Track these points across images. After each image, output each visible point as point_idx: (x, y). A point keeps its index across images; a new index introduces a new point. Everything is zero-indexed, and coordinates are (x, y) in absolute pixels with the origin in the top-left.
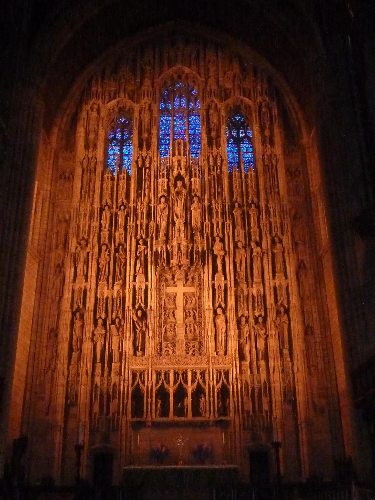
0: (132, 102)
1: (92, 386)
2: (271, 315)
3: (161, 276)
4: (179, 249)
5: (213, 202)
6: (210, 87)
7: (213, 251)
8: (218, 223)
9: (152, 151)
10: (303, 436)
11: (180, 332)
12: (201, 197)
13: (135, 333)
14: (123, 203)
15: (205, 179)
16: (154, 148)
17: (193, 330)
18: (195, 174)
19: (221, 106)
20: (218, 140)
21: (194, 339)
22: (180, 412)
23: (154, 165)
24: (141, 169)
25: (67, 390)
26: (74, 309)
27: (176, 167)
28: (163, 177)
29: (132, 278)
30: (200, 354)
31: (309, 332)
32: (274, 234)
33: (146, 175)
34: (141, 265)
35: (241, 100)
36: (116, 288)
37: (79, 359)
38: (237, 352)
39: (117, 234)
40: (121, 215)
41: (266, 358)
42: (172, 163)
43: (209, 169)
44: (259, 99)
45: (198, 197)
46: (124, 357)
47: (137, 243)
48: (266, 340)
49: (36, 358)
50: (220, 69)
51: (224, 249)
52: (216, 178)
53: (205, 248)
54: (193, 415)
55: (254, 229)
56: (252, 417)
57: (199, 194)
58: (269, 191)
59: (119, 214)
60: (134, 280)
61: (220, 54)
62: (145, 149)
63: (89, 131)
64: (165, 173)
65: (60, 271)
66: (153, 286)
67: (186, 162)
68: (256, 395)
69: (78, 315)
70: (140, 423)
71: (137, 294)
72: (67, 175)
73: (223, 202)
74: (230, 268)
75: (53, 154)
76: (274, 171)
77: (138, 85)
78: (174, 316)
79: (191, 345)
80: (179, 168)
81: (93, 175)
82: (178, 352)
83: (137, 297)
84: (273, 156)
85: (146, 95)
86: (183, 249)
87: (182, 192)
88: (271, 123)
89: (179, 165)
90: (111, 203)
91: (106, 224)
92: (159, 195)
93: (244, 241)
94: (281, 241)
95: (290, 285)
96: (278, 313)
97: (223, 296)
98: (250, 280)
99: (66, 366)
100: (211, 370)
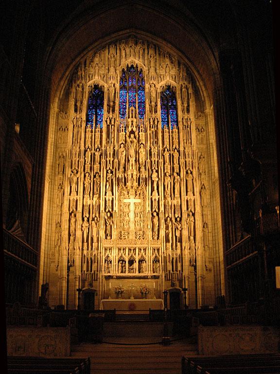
1: (82, 255)
2: (185, 216)
3: (121, 192)
4: (132, 177)
5: (152, 148)
7: (152, 178)
8: (155, 161)
10: (199, 284)
11: (132, 225)
13: (106, 226)
17: (139, 225)
18: (142, 130)
21: (140, 230)
25: (68, 258)
26: (70, 212)
28: (122, 131)
29: (104, 194)
30: (143, 239)
31: (205, 227)
32: (187, 168)
34: (109, 185)
37: (74, 240)
38: (165, 238)
39: (95, 166)
40: (97, 154)
41: (181, 241)
43: (150, 127)
44: (181, 83)
45: (143, 144)
46: (100, 240)
47: (107, 172)
48: (181, 231)
49: (50, 239)
50: (157, 61)
51: (158, 177)
53: (147, 176)
54: (139, 272)
55: (176, 166)
56: (172, 274)
57: (144, 143)
58: (185, 141)
59: (96, 154)
60: (105, 195)
62: (111, 113)
65: (62, 188)
66: (116, 199)
68: (174, 261)
69: (73, 214)
71: (107, 203)
74: (161, 188)
75: (55, 115)
76: (189, 129)
78: (128, 216)
79: (138, 233)
82: (131, 237)
83: (107, 205)
84: (188, 119)
85: (112, 78)
86: (135, 177)
88: (188, 99)
89: (132, 124)
91: (88, 159)
92: (120, 143)
93: (170, 172)
94: (191, 173)
95: (196, 199)
96: (188, 215)
97: (157, 205)
98: (173, 195)
99: (67, 244)
100: (149, 248)
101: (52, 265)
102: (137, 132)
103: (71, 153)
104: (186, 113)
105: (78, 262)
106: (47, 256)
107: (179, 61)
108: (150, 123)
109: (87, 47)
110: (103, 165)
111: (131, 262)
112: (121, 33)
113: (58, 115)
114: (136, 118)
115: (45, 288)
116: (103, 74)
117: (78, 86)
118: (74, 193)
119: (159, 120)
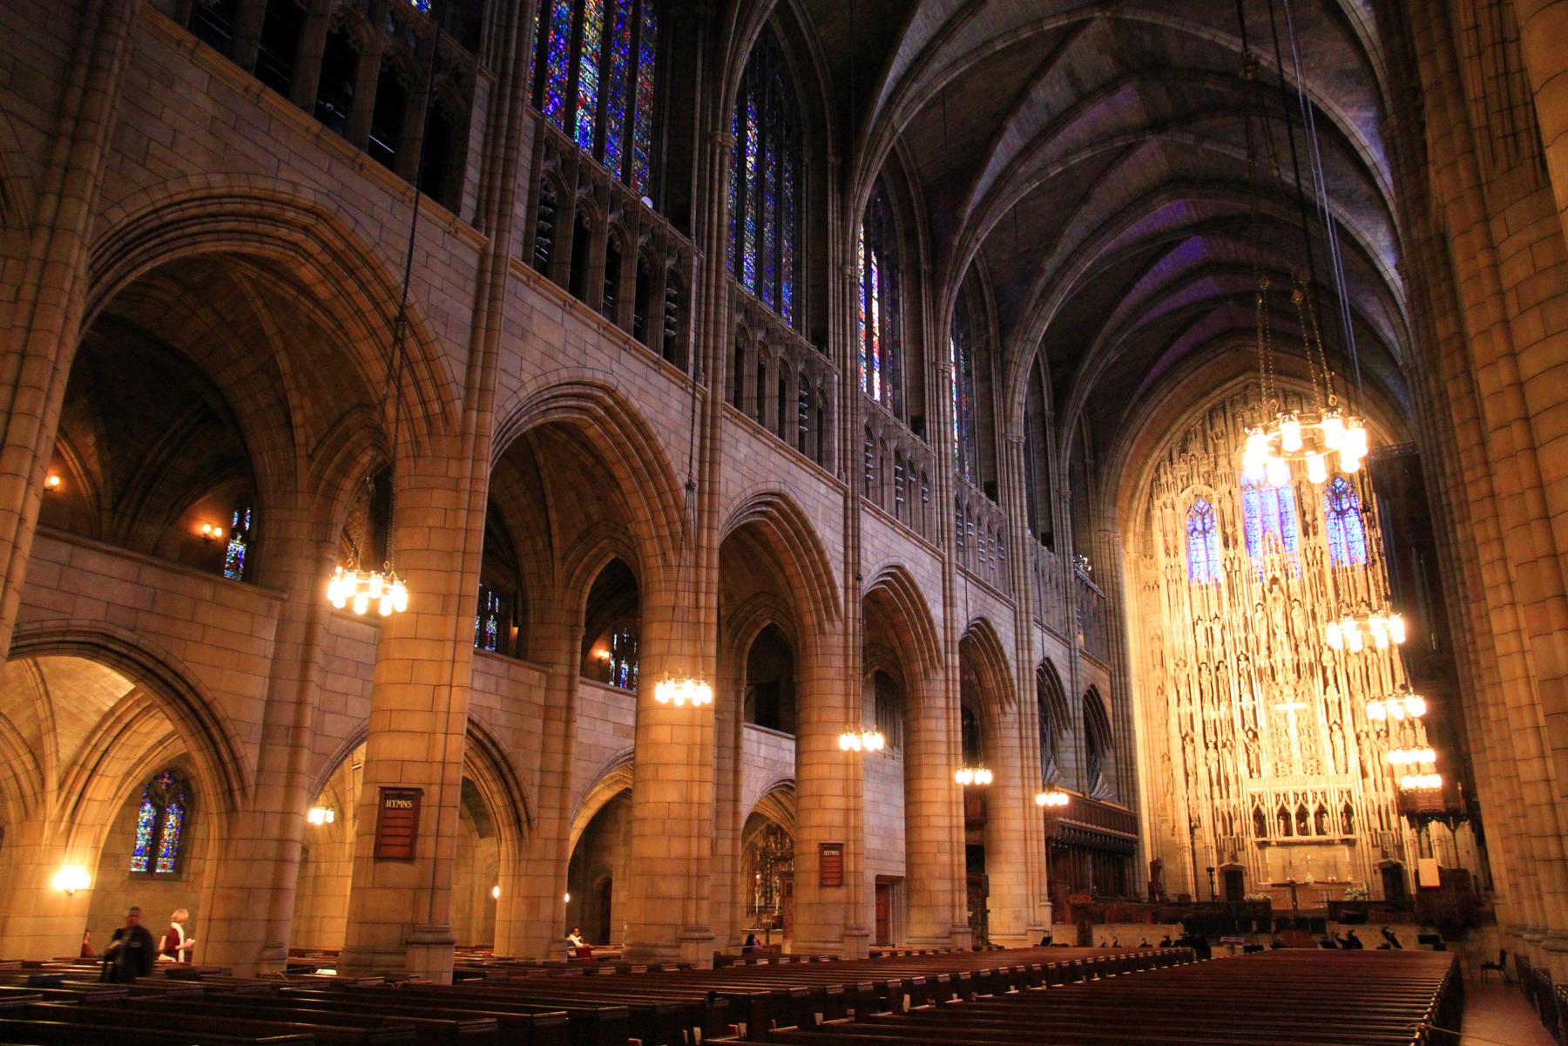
11: (1295, 749)
22: (1304, 831)
23: (1244, 568)
36: (1223, 707)
39: (1215, 650)
47: (1238, 660)
54: (1318, 834)
57: (1299, 598)
70: (1264, 842)
74: (1342, 680)
79: (1308, 764)
82: (1295, 773)
92: (1255, 603)
101: (1164, 826)
103: (1171, 632)
105: (1206, 822)
106: (1153, 811)
109: (1168, 429)
110: (1229, 647)
111: (1302, 814)
112: (1229, 385)
113: (1136, 563)
114: (1277, 552)
115: (1156, 866)
116: (1208, 472)
117: (1164, 504)
118: (1184, 700)
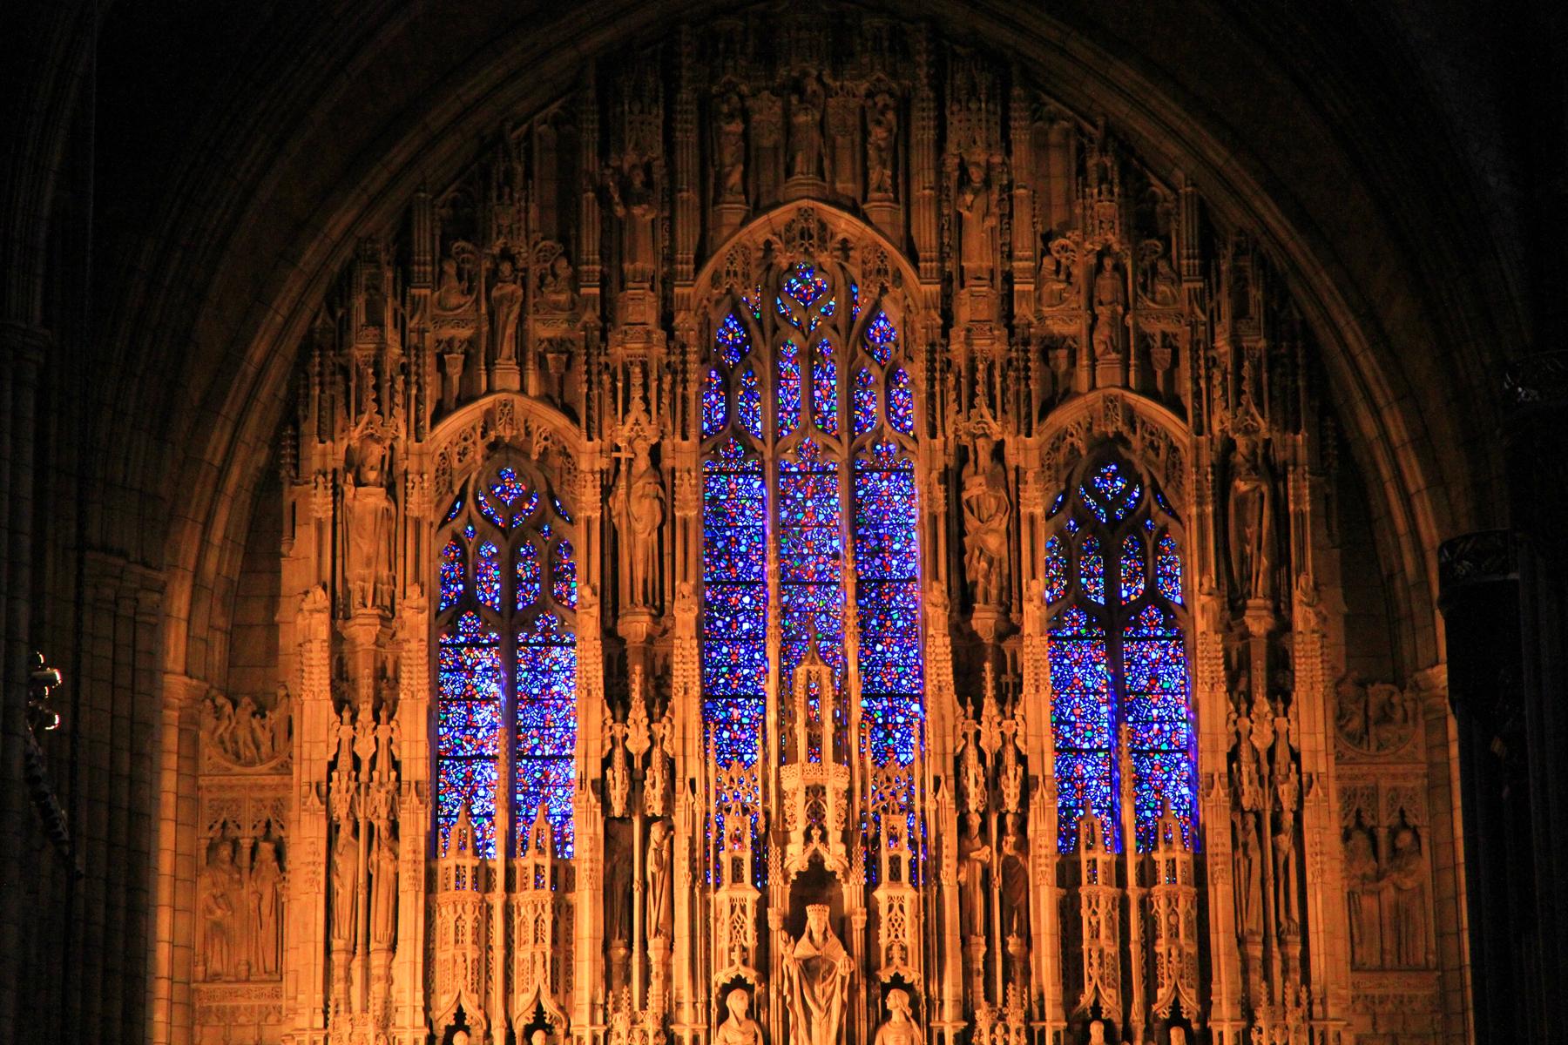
0: (559, 420)
5: (983, 1017)
6: (968, 341)
9: (677, 722)
12: (920, 988)
14: (539, 1012)
15: (940, 887)
16: (687, 706)
18: (895, 861)
19: (1025, 452)
20: (1008, 646)
24: (625, 820)
27: (801, 826)
28: (737, 877)
33: (651, 855)
35: (1131, 416)
42: (781, 795)
44: (1221, 420)
45: (909, 988)
50: (1022, 216)
52: (997, 882)
57: (912, 975)
58: (1256, 951)
61: (1021, 137)
62: (638, 712)
63: (348, 593)
64: (747, 856)
67: (849, 794)
72: (246, 843)
73: (1029, 1017)
76: (1285, 841)
77: (590, 316)
80: (816, 833)
81: (386, 853)
84: (1282, 755)
85: (637, 394)
87: (832, 966)
88: (1281, 559)
89: (816, 814)
90: (479, 1015)
92: (721, 977)
102: (858, 879)
104: (1263, 705)
107: (1202, 203)
108: (961, 796)
116: (559, 346)
117: (353, 464)
119: (1034, 770)
